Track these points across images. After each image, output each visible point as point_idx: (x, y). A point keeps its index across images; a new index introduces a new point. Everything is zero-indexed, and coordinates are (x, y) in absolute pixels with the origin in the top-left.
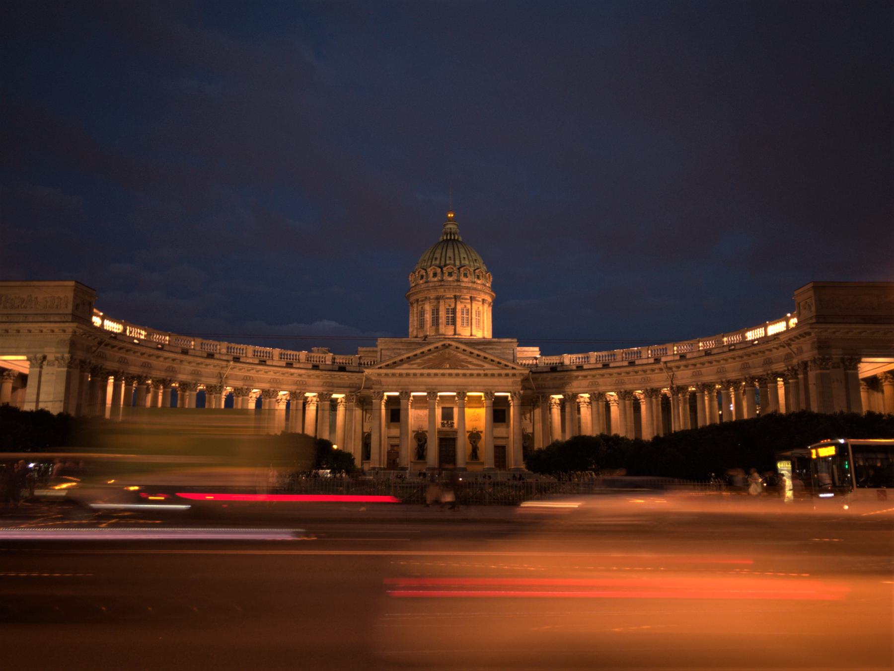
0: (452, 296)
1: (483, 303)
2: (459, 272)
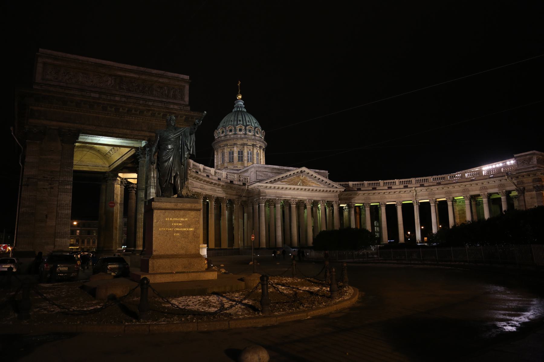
0: (251, 144)
1: (263, 151)
2: (255, 130)
